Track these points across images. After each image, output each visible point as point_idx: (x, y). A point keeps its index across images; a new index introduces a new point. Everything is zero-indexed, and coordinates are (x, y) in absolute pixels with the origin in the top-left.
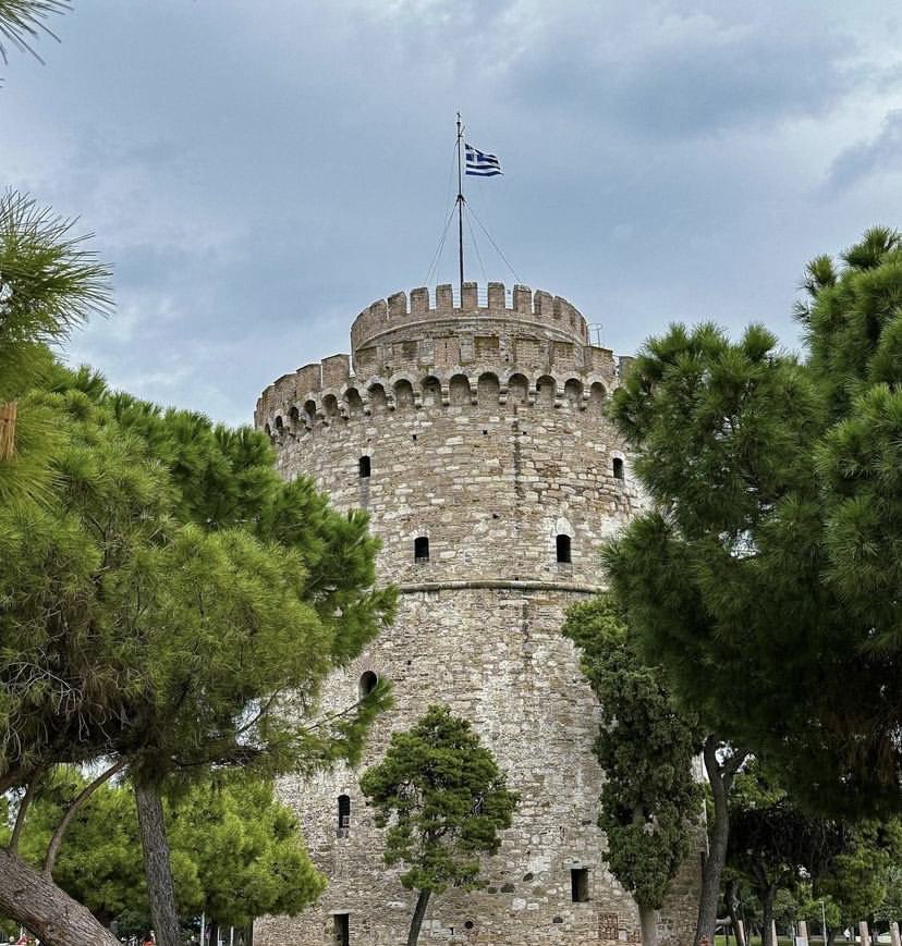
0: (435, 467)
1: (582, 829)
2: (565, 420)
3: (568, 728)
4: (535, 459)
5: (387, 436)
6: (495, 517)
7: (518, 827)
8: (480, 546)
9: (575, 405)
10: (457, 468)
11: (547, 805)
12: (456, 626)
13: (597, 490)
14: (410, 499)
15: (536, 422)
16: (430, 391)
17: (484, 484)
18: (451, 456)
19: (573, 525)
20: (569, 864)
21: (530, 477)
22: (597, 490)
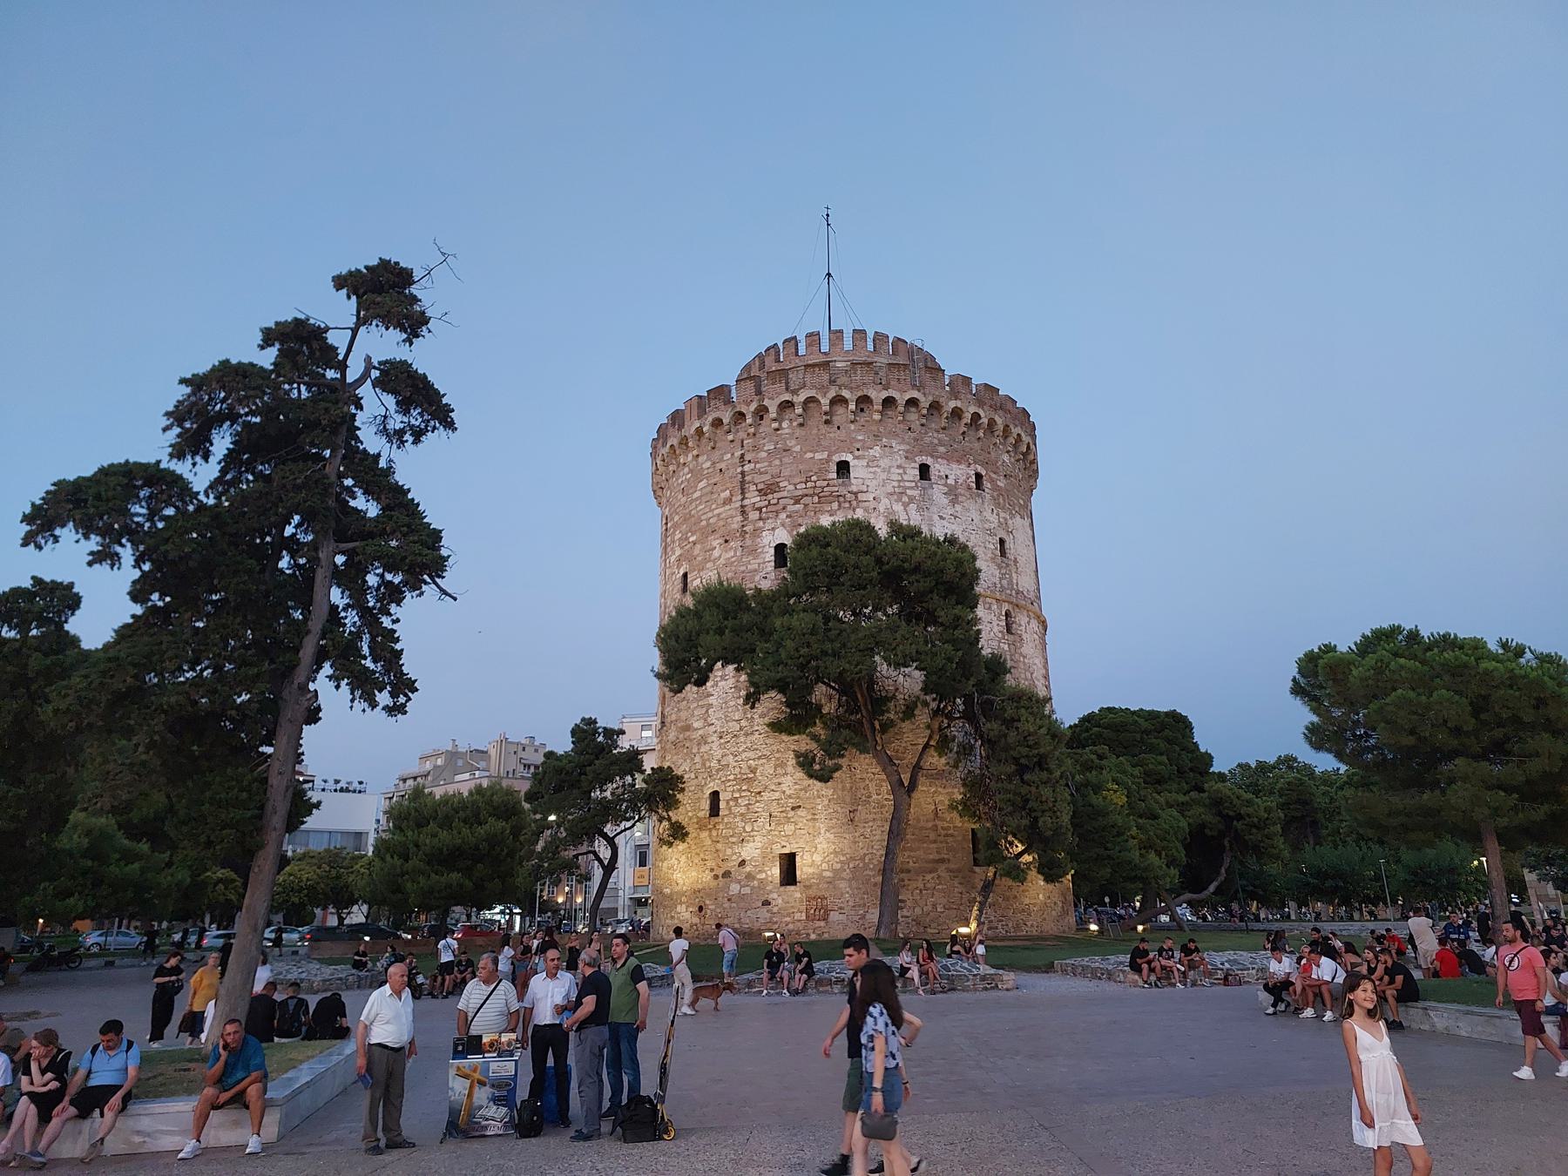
2: (785, 440)
7: (735, 817)
11: (760, 793)
15: (756, 448)
21: (753, 498)
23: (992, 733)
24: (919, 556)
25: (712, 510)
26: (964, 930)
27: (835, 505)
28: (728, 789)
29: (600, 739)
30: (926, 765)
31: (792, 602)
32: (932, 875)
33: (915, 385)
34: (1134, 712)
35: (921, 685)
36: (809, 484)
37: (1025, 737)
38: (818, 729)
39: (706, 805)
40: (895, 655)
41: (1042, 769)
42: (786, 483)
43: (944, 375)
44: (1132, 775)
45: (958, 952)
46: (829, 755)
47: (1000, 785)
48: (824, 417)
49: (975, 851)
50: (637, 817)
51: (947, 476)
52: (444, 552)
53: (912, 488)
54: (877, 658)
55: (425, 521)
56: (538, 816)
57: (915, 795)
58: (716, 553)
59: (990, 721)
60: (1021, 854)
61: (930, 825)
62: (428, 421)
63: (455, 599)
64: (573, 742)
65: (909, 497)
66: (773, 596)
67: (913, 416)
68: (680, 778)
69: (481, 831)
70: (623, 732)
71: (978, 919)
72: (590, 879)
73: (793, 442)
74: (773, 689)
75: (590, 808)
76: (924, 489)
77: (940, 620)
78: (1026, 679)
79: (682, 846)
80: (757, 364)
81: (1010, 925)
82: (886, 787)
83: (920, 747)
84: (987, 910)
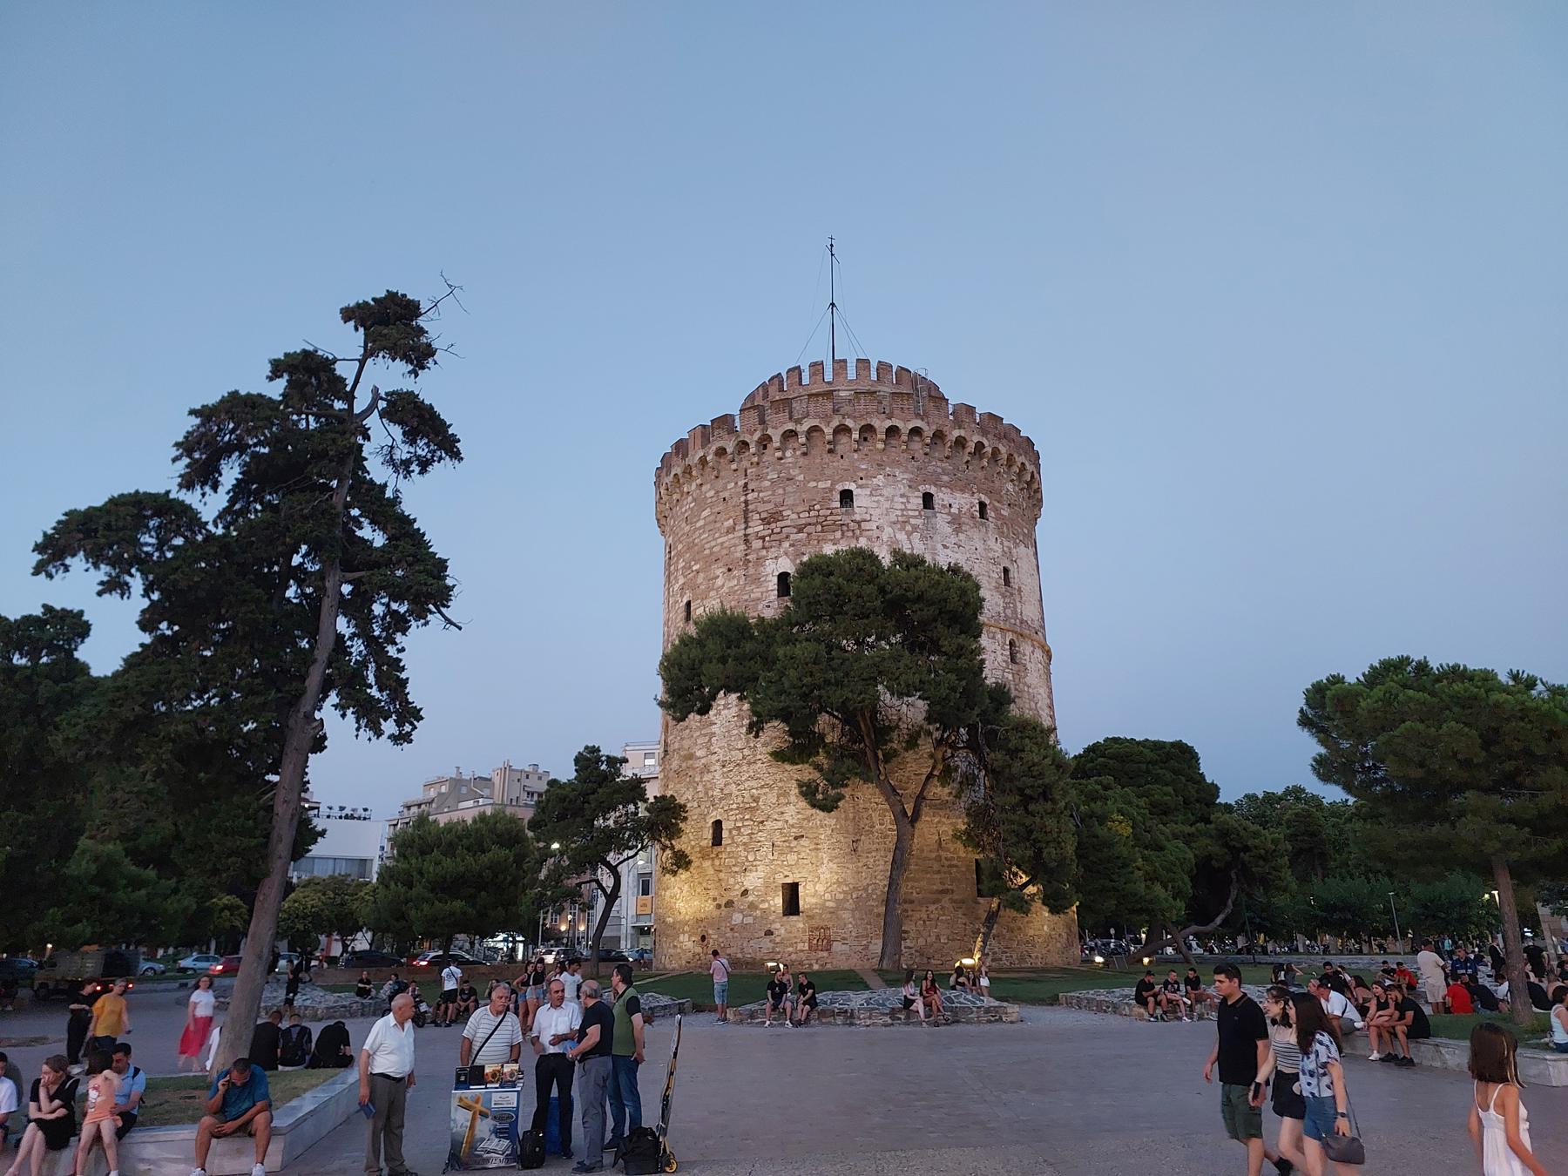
6: (729, 570)
7: (738, 846)
11: (762, 822)
15: (759, 477)
21: (756, 527)
23: (996, 763)
24: (922, 584)
25: (716, 539)
26: (967, 962)
27: (838, 534)
28: (731, 818)
29: (604, 767)
30: (930, 796)
31: (795, 630)
32: (936, 906)
33: (919, 414)
34: (1139, 743)
35: (924, 714)
36: (812, 513)
37: (1029, 768)
38: (821, 758)
39: (708, 834)
40: (899, 684)
41: (1046, 800)
42: (789, 512)
43: (947, 404)
44: (1137, 806)
45: (963, 984)
46: (832, 785)
47: (1004, 815)
49: (979, 881)
50: (640, 846)
51: (950, 505)
52: (449, 582)
53: (915, 517)
54: (880, 687)
55: (431, 550)
56: (541, 845)
57: (918, 825)
58: (719, 582)
59: (994, 751)
60: (1025, 885)
61: (933, 855)
62: (435, 451)
63: (460, 628)
64: (576, 770)
65: (913, 526)
66: (776, 624)
67: (916, 445)
68: (682, 807)
69: (485, 859)
70: (626, 761)
71: (982, 950)
72: (592, 908)
73: (797, 471)
74: (776, 719)
75: (592, 837)
76: (928, 518)
77: (943, 650)
78: (1030, 709)
79: (683, 875)
80: (761, 393)
81: (1015, 956)
82: (889, 817)
83: (924, 777)
84: (991, 941)
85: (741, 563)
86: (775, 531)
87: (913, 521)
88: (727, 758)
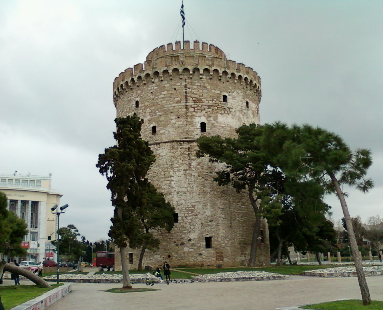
0: (158, 102)
1: (209, 223)
2: (204, 83)
3: (205, 189)
4: (192, 97)
5: (144, 93)
6: (178, 117)
8: (173, 128)
9: (208, 78)
10: (166, 102)
11: (197, 215)
12: (165, 156)
13: (217, 106)
14: (151, 113)
15: (192, 84)
16: (157, 77)
17: (174, 107)
18: (164, 97)
19: (207, 119)
20: (205, 235)
21: (191, 103)
22: (217, 106)
27: (223, 111)
36: (213, 102)
48: (220, 78)
53: (244, 110)
85: (184, 116)
86: (199, 106)
87: (244, 111)
88: (180, 191)
